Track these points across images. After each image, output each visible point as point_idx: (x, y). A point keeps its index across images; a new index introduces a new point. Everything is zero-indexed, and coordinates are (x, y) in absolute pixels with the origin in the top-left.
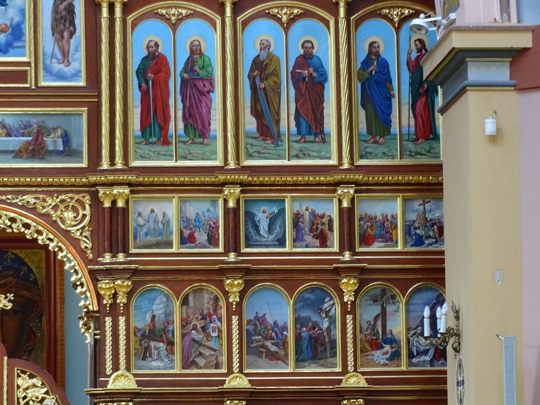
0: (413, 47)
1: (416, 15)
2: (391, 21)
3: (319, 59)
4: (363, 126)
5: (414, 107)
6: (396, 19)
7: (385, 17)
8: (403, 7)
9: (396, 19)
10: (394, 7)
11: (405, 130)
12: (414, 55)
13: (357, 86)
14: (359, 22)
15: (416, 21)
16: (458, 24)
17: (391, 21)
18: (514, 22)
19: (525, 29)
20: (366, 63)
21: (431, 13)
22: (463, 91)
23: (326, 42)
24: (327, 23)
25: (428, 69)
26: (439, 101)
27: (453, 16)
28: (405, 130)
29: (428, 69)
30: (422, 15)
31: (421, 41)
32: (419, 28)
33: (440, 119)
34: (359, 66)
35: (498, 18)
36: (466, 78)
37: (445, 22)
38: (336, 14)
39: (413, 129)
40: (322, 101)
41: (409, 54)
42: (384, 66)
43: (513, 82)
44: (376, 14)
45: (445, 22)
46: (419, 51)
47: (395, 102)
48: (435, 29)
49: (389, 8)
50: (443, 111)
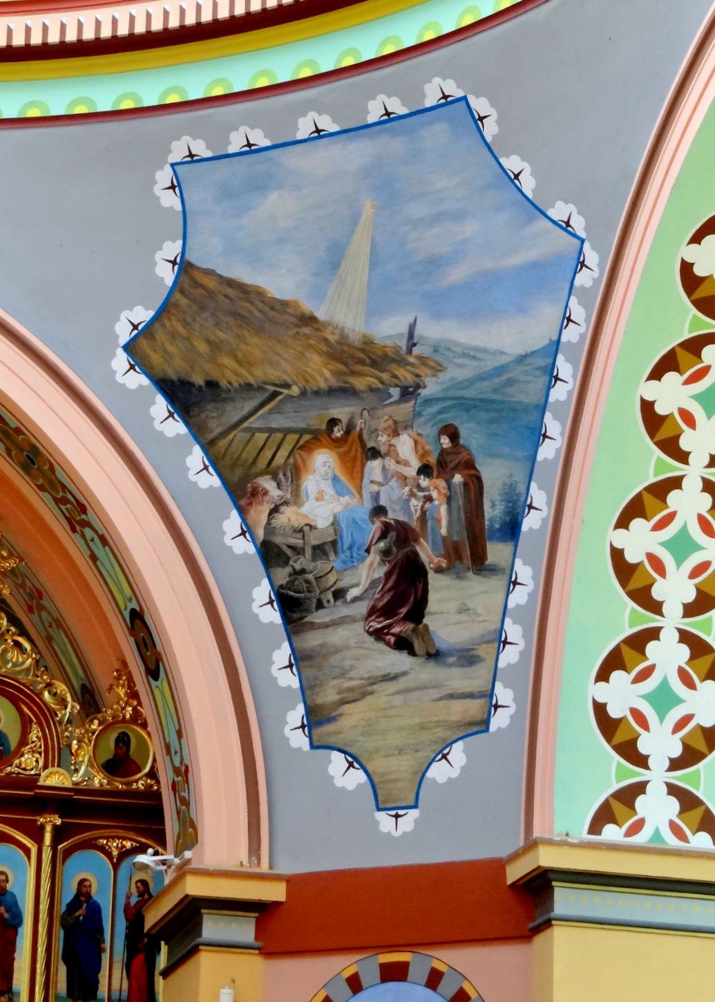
0: (134, 890)
1: (142, 849)
2: (108, 854)
3: (13, 896)
4: (61, 985)
5: (128, 966)
6: (115, 853)
7: (102, 849)
8: (124, 839)
9: (115, 853)
10: (113, 838)
11: (115, 996)
12: (134, 900)
13: (59, 934)
14: (68, 853)
15: (141, 858)
16: (193, 865)
17: (108, 854)
18: (264, 868)
19: (277, 878)
20: (73, 905)
21: (160, 850)
22: (195, 950)
23: (25, 874)
24: (27, 851)
25: (152, 918)
26: (162, 961)
27: (188, 854)
28: (115, 996)
29: (152, 918)
30: (150, 851)
31: (144, 883)
32: (145, 867)
33: (160, 984)
34: (64, 908)
35: (245, 861)
36: (200, 935)
37: (177, 861)
38: (39, 840)
39: (125, 994)
40: (14, 951)
41: (128, 897)
42: (95, 910)
43: (259, 944)
44: (90, 845)
45: (177, 861)
46: (141, 894)
47: (105, 958)
48: (164, 868)
49: (107, 838)
50: (166, 973)
